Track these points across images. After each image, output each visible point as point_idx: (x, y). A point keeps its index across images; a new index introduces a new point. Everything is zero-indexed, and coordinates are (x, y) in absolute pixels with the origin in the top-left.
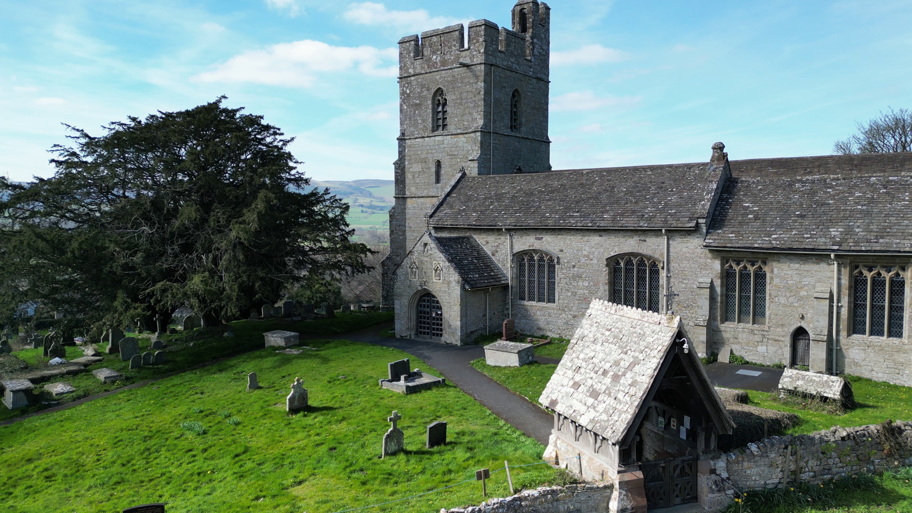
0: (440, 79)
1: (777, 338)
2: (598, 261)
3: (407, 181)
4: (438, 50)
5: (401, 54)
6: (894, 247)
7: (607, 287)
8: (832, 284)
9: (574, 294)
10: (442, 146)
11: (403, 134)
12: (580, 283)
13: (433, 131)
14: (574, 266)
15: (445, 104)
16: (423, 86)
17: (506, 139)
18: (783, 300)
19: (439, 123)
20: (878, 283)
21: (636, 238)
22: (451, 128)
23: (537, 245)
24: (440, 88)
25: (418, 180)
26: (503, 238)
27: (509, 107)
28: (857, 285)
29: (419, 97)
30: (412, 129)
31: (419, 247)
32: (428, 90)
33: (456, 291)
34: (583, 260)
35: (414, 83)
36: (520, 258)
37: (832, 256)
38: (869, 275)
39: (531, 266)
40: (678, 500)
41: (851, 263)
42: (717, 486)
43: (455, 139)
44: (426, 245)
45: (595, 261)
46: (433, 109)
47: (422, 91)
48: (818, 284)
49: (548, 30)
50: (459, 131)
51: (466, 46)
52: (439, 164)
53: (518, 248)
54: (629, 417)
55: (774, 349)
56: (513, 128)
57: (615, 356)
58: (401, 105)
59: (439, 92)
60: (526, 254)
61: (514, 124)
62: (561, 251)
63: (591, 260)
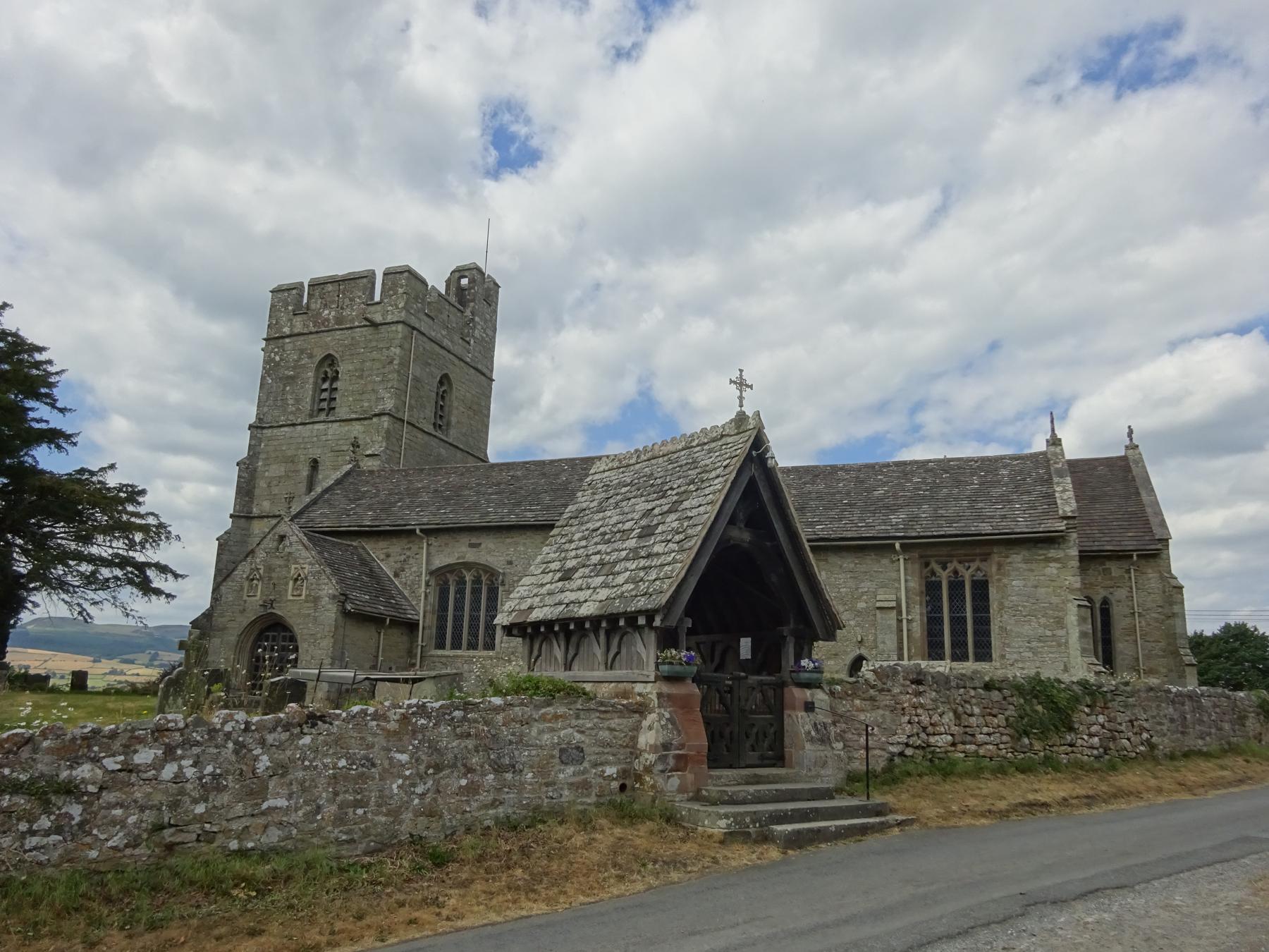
0: (331, 343)
3: (257, 492)
4: (333, 302)
5: (273, 306)
6: (973, 530)
8: (899, 589)
10: (324, 438)
11: (259, 419)
13: (311, 416)
15: (335, 378)
16: (302, 351)
17: (426, 438)
19: (325, 406)
20: (956, 587)
22: (342, 412)
23: (470, 556)
24: (329, 355)
25: (275, 490)
26: (415, 548)
27: (434, 395)
28: (931, 589)
29: (294, 368)
30: (276, 413)
31: (270, 543)
32: (311, 356)
33: (330, 613)
35: (289, 347)
36: (441, 575)
37: (897, 546)
38: (944, 576)
39: (460, 592)
40: (753, 756)
41: (921, 557)
42: (817, 730)
43: (346, 428)
44: (282, 538)
46: (315, 383)
47: (300, 359)
48: (881, 591)
49: (495, 312)
50: (354, 416)
51: (377, 298)
52: (315, 465)
53: (439, 561)
54: (679, 570)
56: (437, 426)
57: (642, 506)
58: (263, 378)
59: (329, 360)
60: (451, 572)
61: (439, 422)
62: (510, 563)
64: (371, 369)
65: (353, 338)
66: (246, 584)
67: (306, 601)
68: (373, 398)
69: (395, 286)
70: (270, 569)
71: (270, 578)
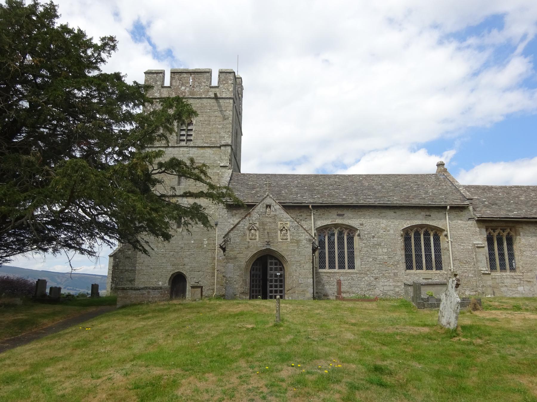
1: (529, 280)
2: (394, 232)
7: (403, 252)
9: (375, 259)
12: (380, 250)
14: (374, 237)
18: (528, 253)
21: (423, 213)
23: (339, 221)
34: (382, 231)
45: (392, 232)
50: (206, 145)
53: (321, 223)
55: (528, 288)
62: (362, 225)
63: (389, 231)
64: (215, 121)
65: (202, 104)
66: (248, 232)
67: (292, 243)
68: (218, 136)
69: (226, 80)
70: (263, 224)
71: (264, 229)
